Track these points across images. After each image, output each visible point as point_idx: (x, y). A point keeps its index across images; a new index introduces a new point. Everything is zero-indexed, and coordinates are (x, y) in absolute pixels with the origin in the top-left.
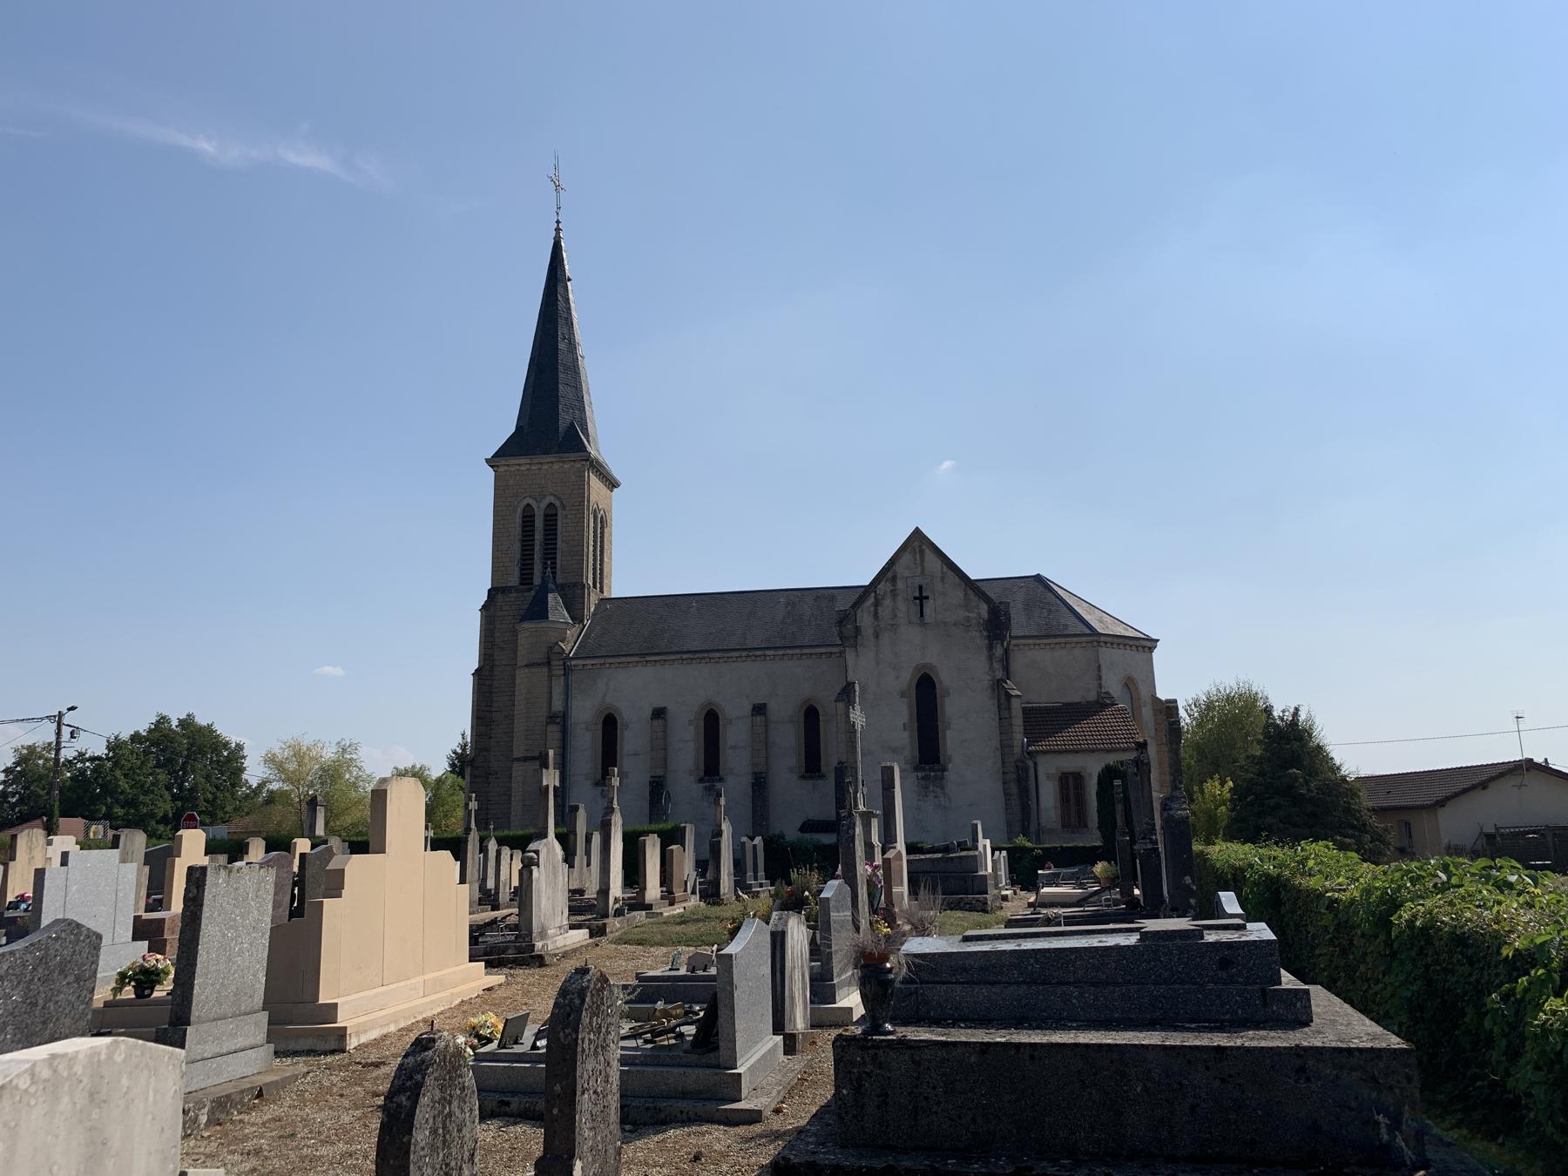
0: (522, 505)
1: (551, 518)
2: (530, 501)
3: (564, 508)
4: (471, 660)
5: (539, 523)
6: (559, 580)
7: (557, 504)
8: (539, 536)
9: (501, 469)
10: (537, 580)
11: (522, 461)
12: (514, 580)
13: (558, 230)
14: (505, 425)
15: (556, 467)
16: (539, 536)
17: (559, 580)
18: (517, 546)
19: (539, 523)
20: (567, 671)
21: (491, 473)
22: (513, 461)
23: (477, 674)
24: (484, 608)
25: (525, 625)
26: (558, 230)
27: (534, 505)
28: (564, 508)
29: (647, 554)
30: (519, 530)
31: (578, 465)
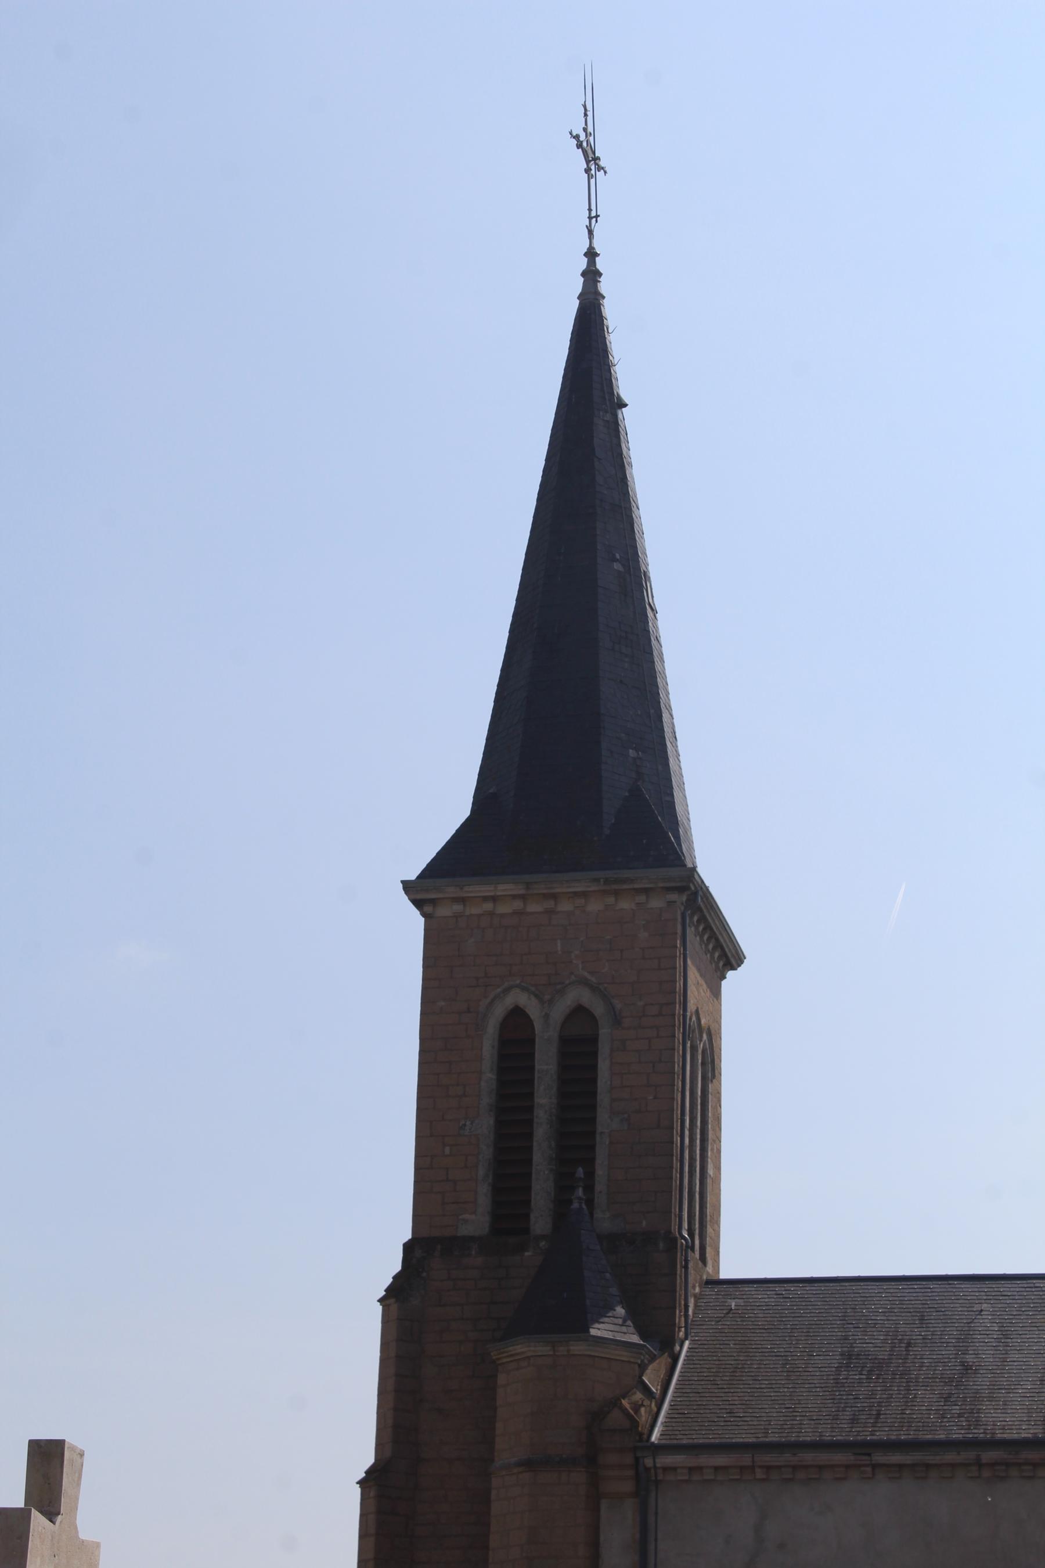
0: (499, 1012)
1: (579, 1048)
2: (523, 999)
3: (617, 1021)
4: (353, 1440)
5: (546, 1062)
6: (604, 1221)
7: (599, 1009)
8: (545, 1098)
9: (444, 911)
10: (540, 1222)
11: (505, 888)
12: (476, 1221)
13: (591, 275)
14: (443, 798)
15: (594, 906)
16: (545, 1098)
17: (604, 1221)
18: (485, 1125)
19: (546, 1062)
20: (646, 1484)
21: (415, 922)
22: (477, 889)
23: (373, 1482)
24: (396, 1295)
25: (520, 1348)
26: (591, 275)
27: (534, 1011)
28: (617, 1021)
29: (838, 1154)
30: (489, 1076)
31: (656, 903)
